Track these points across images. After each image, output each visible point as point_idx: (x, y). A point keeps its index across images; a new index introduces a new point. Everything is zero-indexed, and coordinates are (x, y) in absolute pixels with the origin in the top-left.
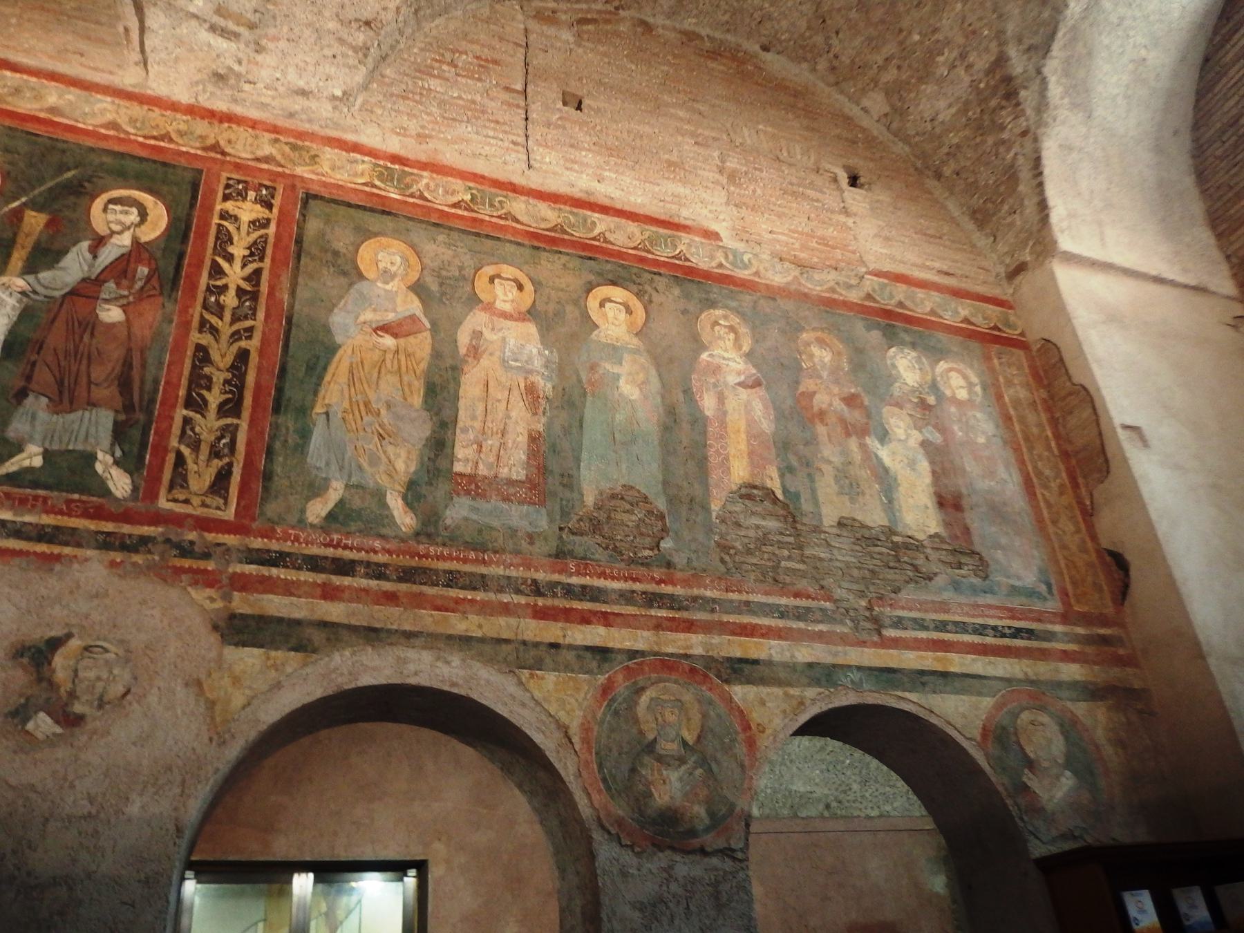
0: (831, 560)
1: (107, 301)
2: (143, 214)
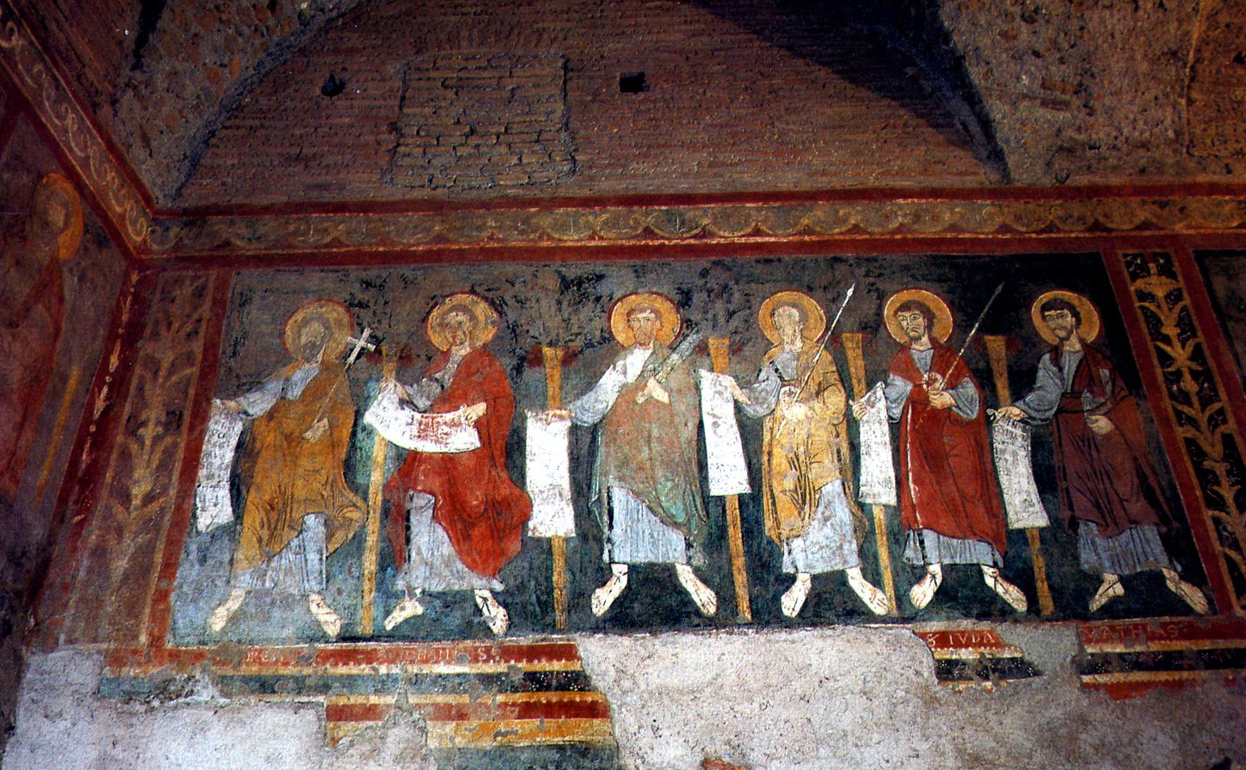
1: (1092, 412)
2: (1076, 314)
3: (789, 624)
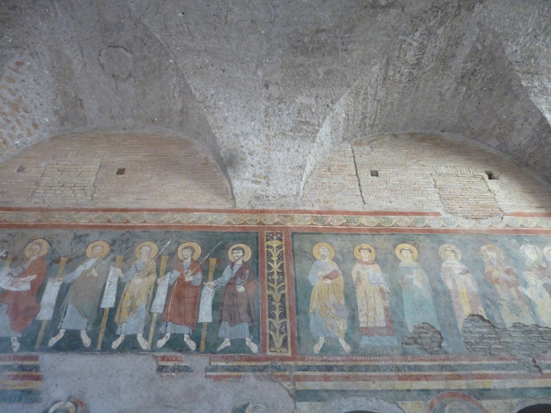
0: (513, 342)
1: (239, 284)
3: (113, 352)
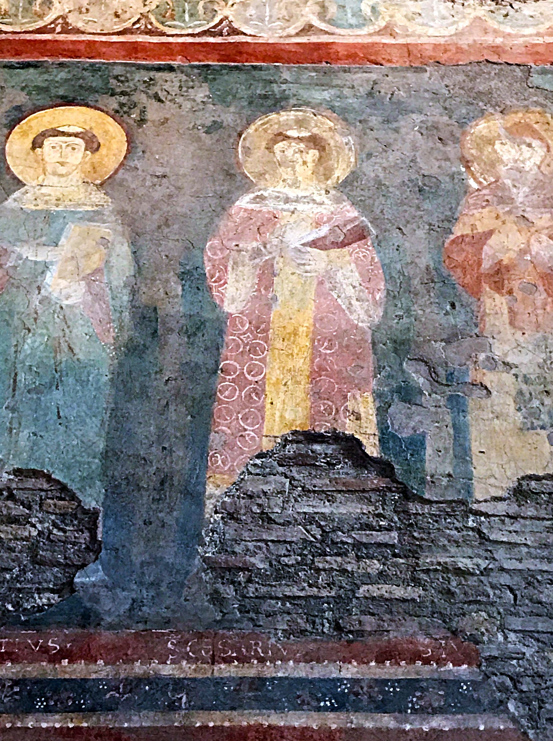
0: (486, 572)
